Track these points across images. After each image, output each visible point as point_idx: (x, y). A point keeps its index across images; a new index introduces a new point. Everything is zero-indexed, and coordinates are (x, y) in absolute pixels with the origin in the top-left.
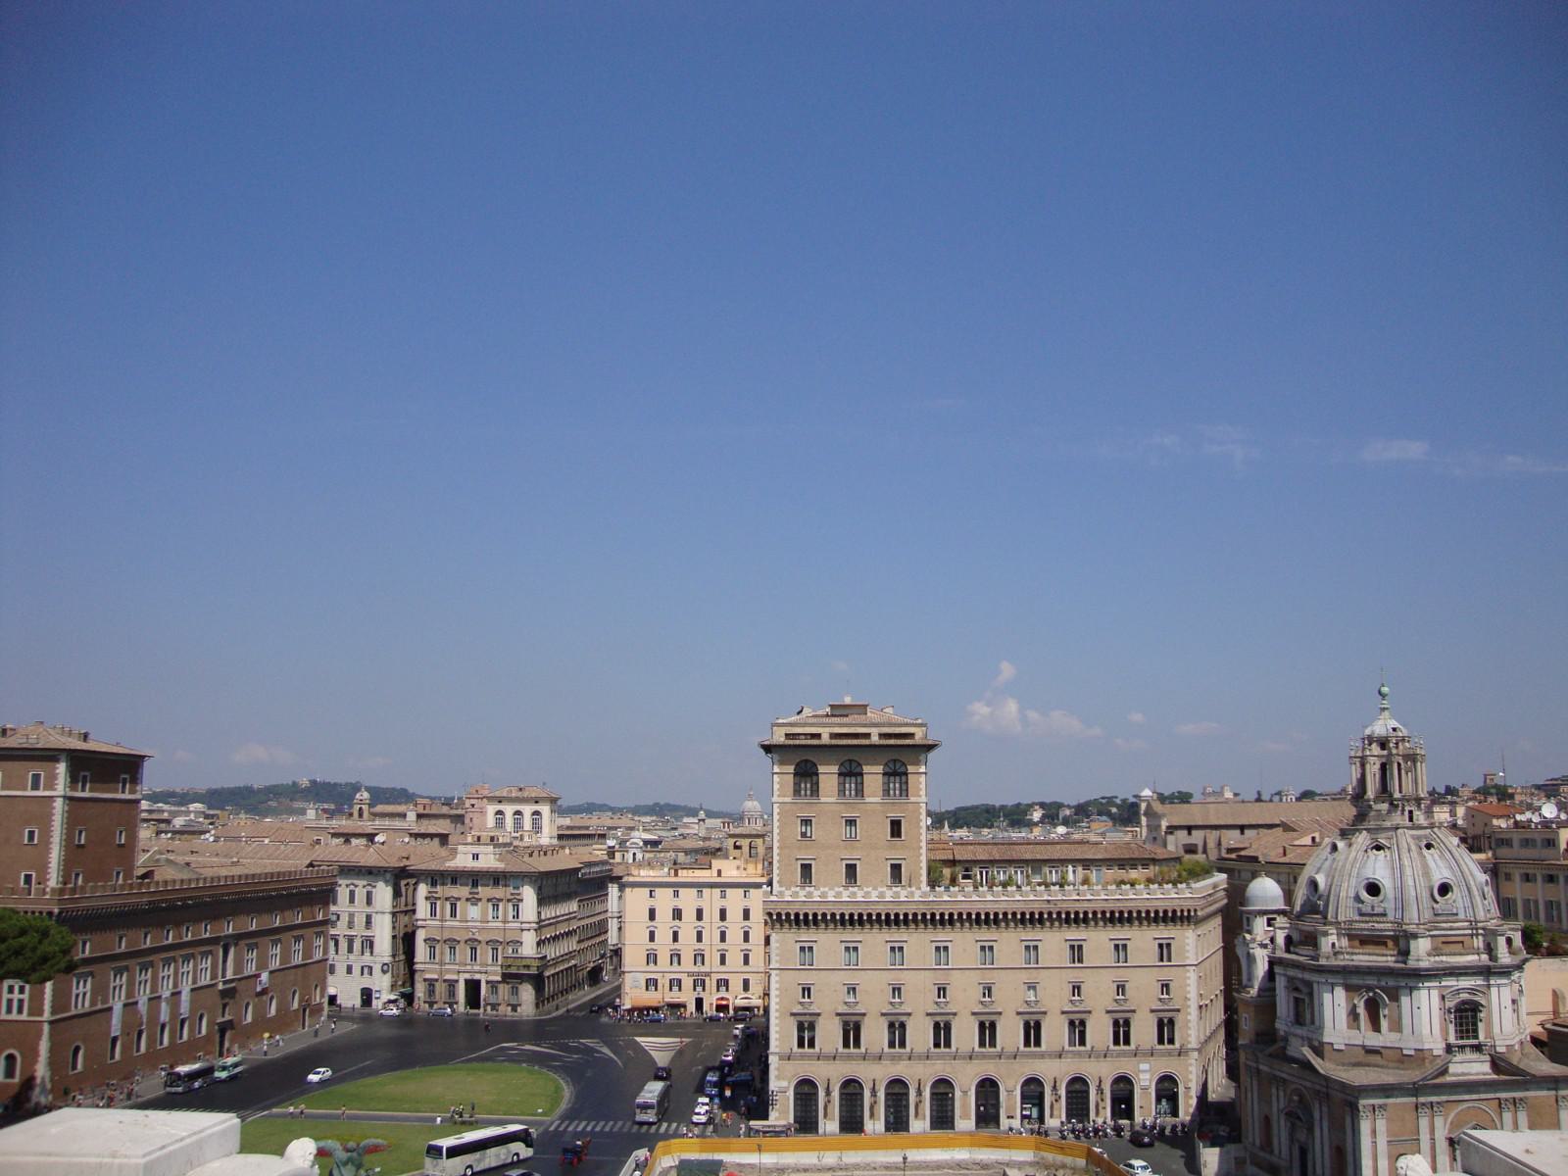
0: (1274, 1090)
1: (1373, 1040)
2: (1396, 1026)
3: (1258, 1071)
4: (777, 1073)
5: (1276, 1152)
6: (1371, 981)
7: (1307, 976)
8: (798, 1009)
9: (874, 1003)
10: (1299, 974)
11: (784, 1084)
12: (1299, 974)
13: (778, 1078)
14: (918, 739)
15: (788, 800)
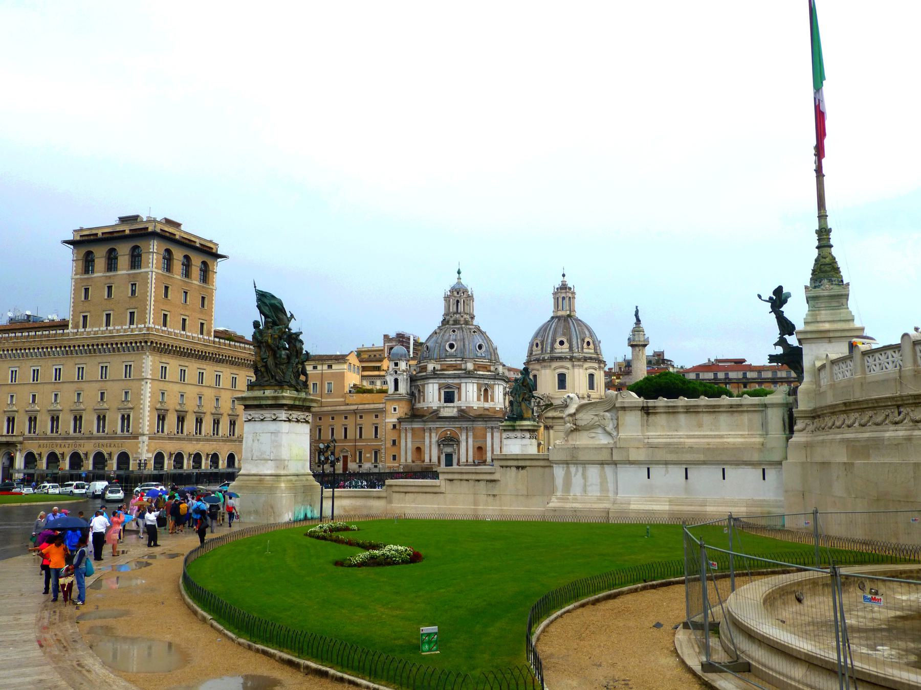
0: (427, 434)
1: (487, 405)
2: (492, 400)
3: (413, 429)
4: (146, 448)
5: (427, 460)
6: (486, 382)
7: (457, 381)
8: (159, 406)
9: (191, 405)
10: (450, 381)
11: (150, 455)
12: (450, 381)
13: (148, 451)
14: (214, 251)
15: (160, 272)
